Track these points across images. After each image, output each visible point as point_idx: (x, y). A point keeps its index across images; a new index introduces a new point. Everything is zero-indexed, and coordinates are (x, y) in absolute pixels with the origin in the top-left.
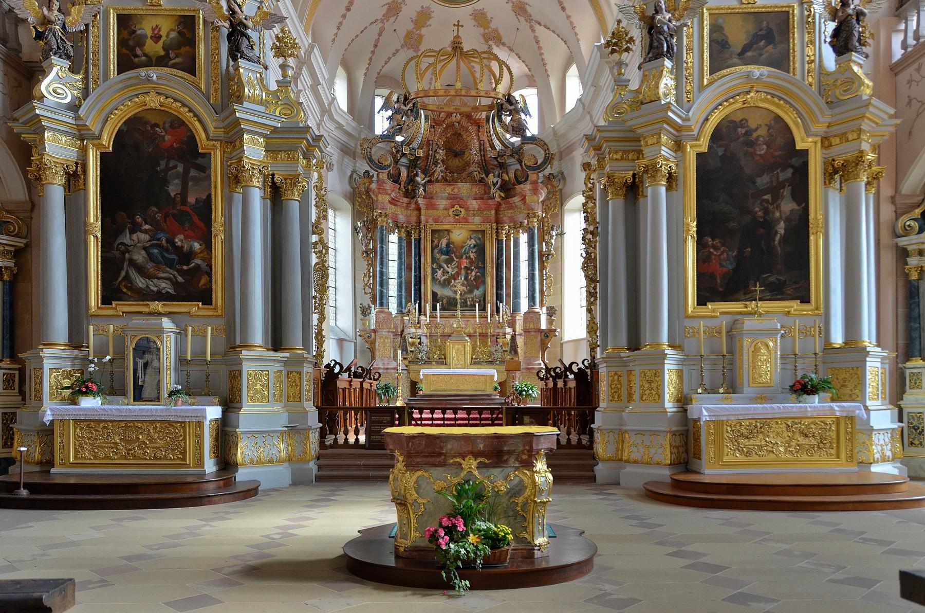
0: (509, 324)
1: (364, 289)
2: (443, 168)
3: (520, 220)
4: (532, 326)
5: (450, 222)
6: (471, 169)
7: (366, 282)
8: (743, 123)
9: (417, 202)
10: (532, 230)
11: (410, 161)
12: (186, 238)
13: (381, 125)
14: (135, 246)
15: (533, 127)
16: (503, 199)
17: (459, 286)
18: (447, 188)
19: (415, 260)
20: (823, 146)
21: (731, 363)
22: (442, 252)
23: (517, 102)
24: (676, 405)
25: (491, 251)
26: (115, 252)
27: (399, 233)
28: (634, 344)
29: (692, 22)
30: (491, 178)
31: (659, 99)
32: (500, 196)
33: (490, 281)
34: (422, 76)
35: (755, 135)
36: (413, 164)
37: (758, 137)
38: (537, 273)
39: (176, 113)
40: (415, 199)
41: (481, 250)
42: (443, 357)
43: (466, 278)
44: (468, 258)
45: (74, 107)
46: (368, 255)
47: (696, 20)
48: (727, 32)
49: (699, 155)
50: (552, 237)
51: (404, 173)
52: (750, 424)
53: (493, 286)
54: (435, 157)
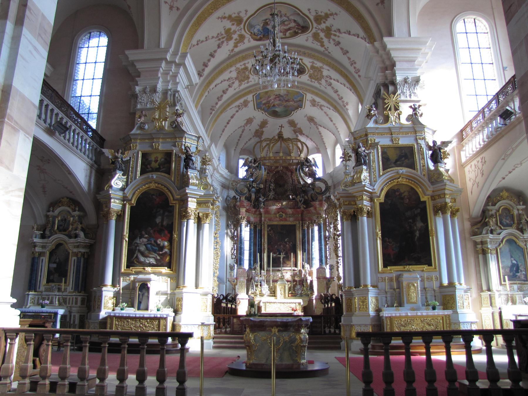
2: (273, 193)
4: (321, 275)
6: (288, 193)
8: (398, 190)
9: (260, 211)
11: (256, 190)
12: (162, 240)
13: (242, 173)
14: (141, 244)
15: (319, 173)
16: (305, 208)
20: (432, 200)
21: (400, 293)
23: (311, 161)
24: (375, 313)
26: (133, 246)
27: (250, 227)
28: (357, 285)
29: (374, 151)
30: (299, 198)
31: (361, 182)
32: (303, 207)
34: (263, 149)
35: (403, 195)
36: (258, 191)
37: (405, 196)
38: (323, 247)
39: (161, 190)
45: (123, 189)
47: (375, 150)
48: (389, 154)
49: (381, 204)
50: (331, 228)
51: (253, 196)
52: (405, 320)
54: (269, 187)
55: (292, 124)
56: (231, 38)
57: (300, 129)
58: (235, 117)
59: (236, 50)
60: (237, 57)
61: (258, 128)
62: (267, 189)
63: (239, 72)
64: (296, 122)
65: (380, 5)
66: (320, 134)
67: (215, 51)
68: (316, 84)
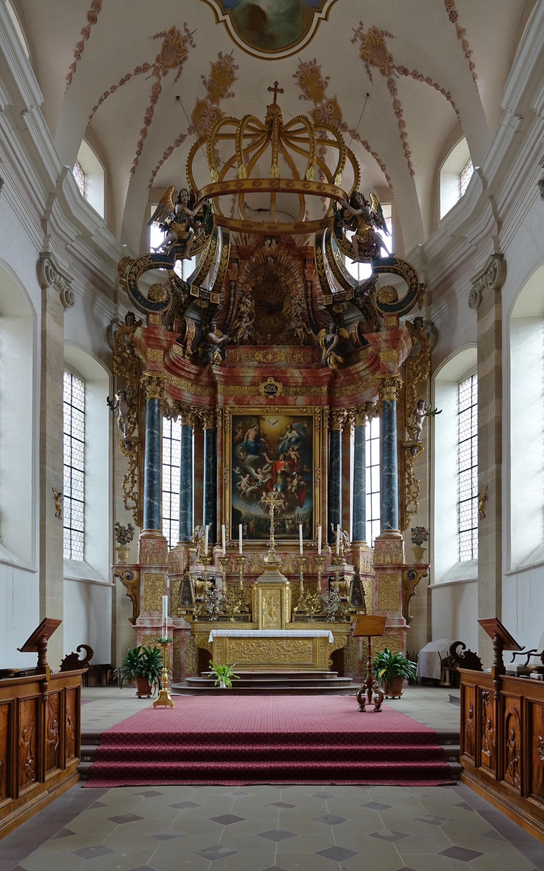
0: (348, 558)
1: (125, 502)
3: (367, 399)
5: (260, 404)
6: (293, 325)
7: (127, 491)
10: (389, 405)
18: (257, 354)
19: (207, 462)
22: (248, 450)
32: (336, 362)
40: (208, 366)
42: (247, 609)
43: (284, 489)
44: (287, 458)
46: (131, 447)
50: (418, 418)
53: (324, 501)
54: (239, 309)
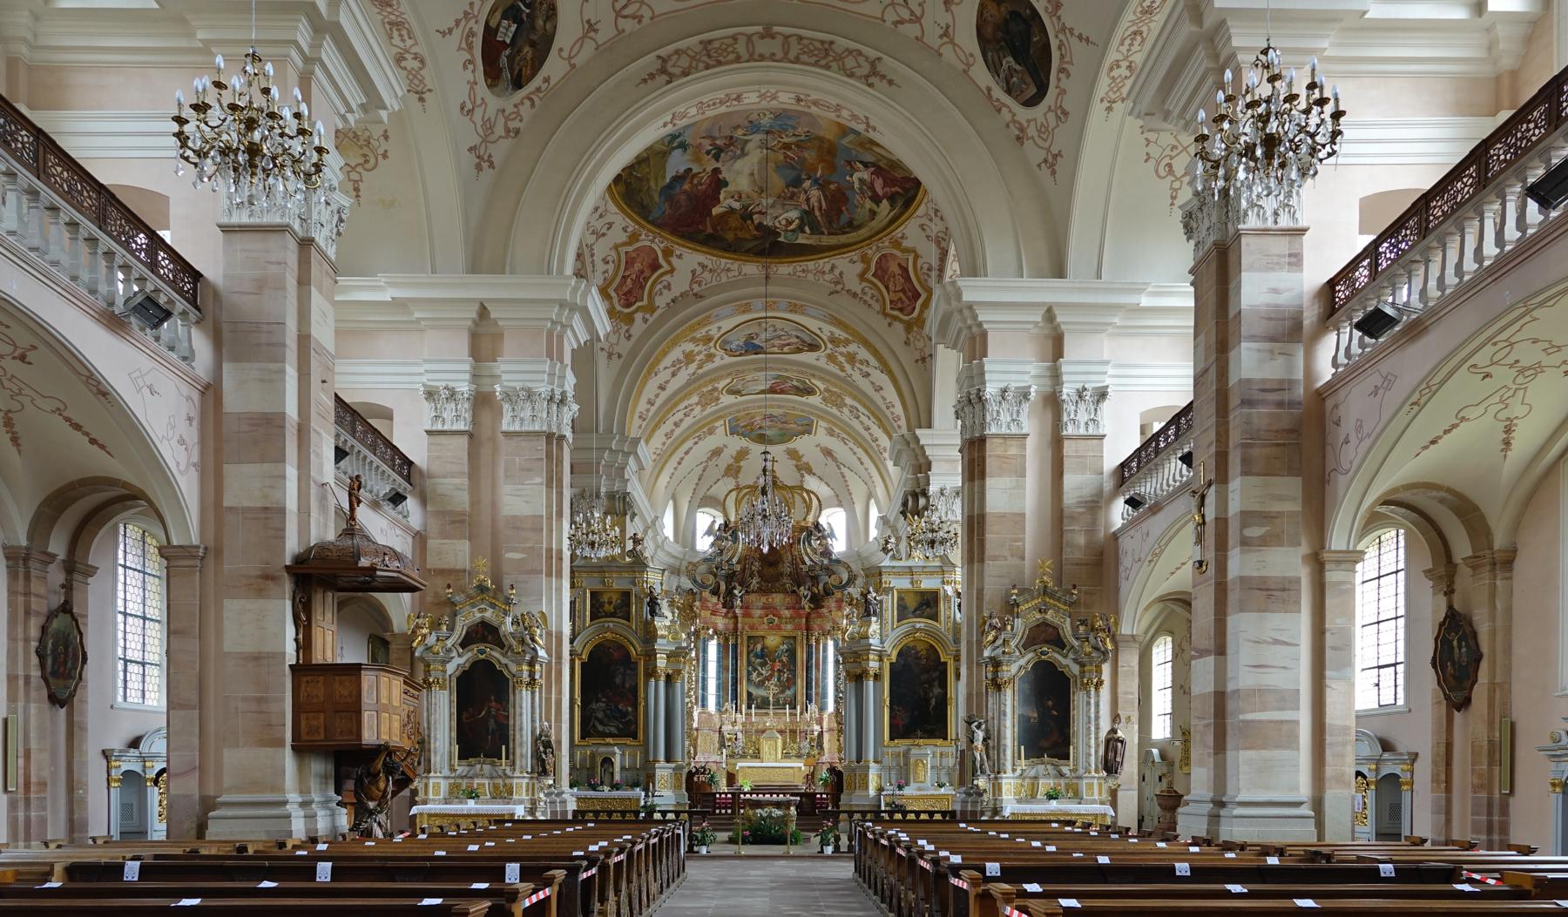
13: (704, 544)
15: (839, 546)
16: (812, 609)
17: (772, 687)
22: (757, 656)
25: (801, 655)
30: (803, 591)
32: (810, 607)
33: (800, 683)
36: (730, 578)
41: (792, 654)
55: (793, 454)
56: (694, 361)
57: (807, 464)
58: (692, 452)
59: (700, 371)
60: (702, 381)
61: (731, 461)
62: (748, 572)
63: (702, 395)
64: (801, 453)
65: (920, 362)
66: (843, 477)
67: (667, 382)
68: (834, 410)
